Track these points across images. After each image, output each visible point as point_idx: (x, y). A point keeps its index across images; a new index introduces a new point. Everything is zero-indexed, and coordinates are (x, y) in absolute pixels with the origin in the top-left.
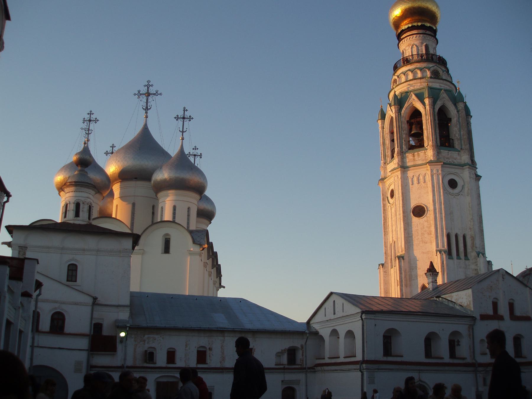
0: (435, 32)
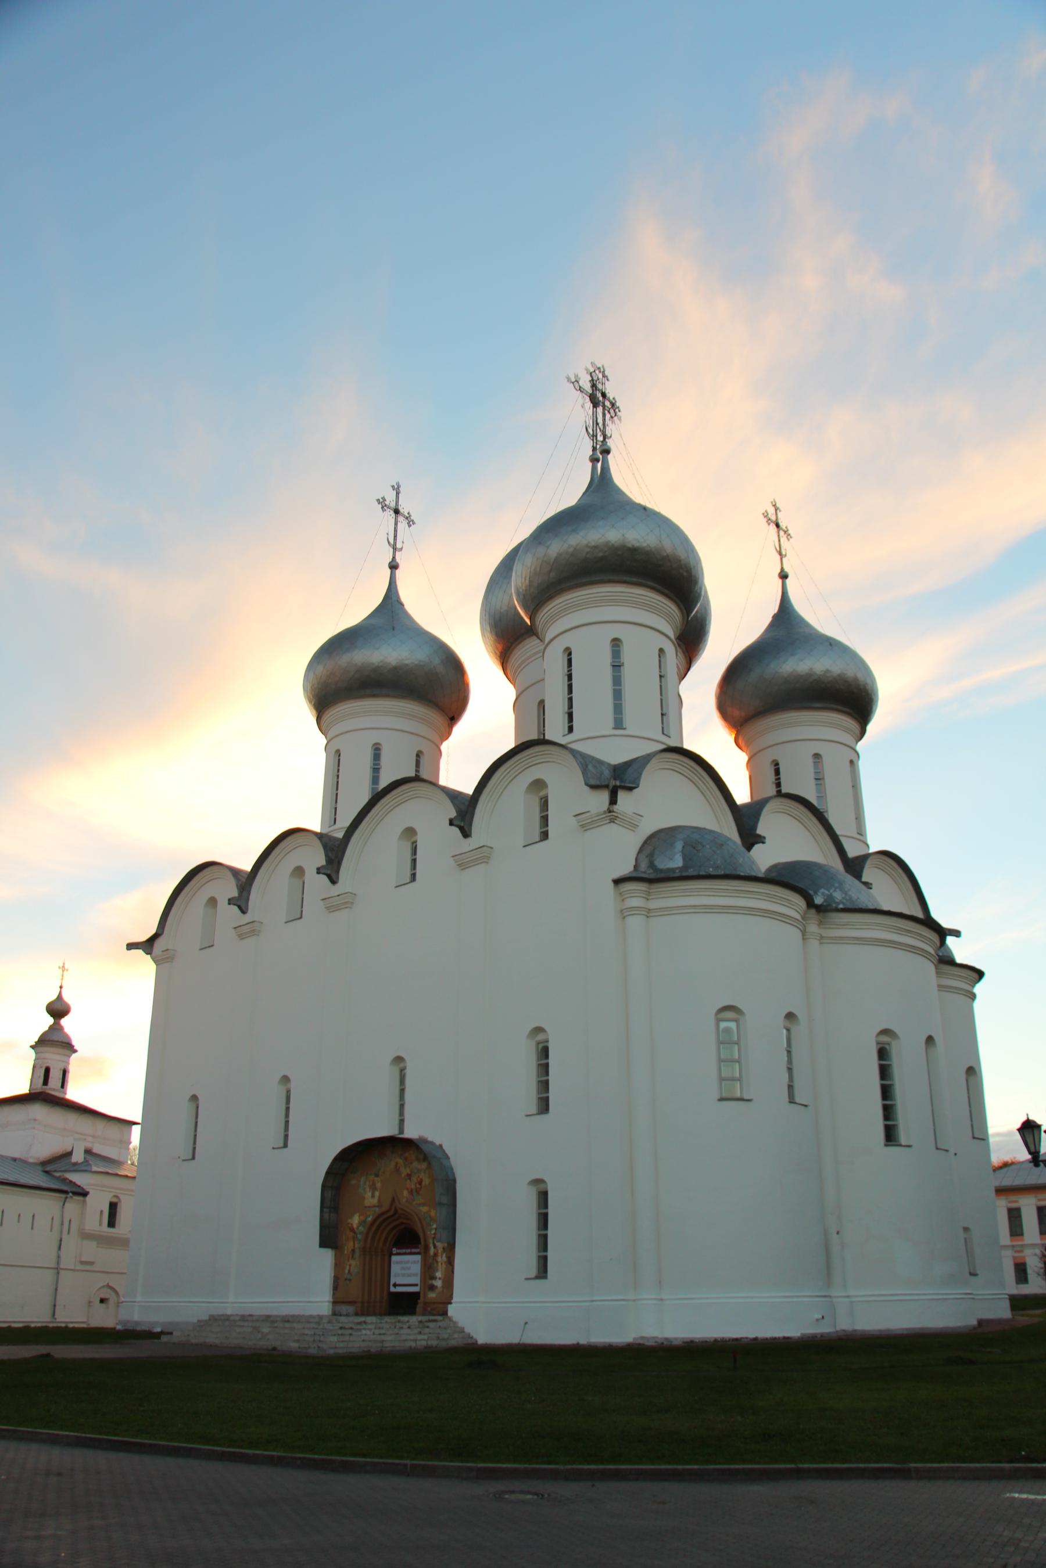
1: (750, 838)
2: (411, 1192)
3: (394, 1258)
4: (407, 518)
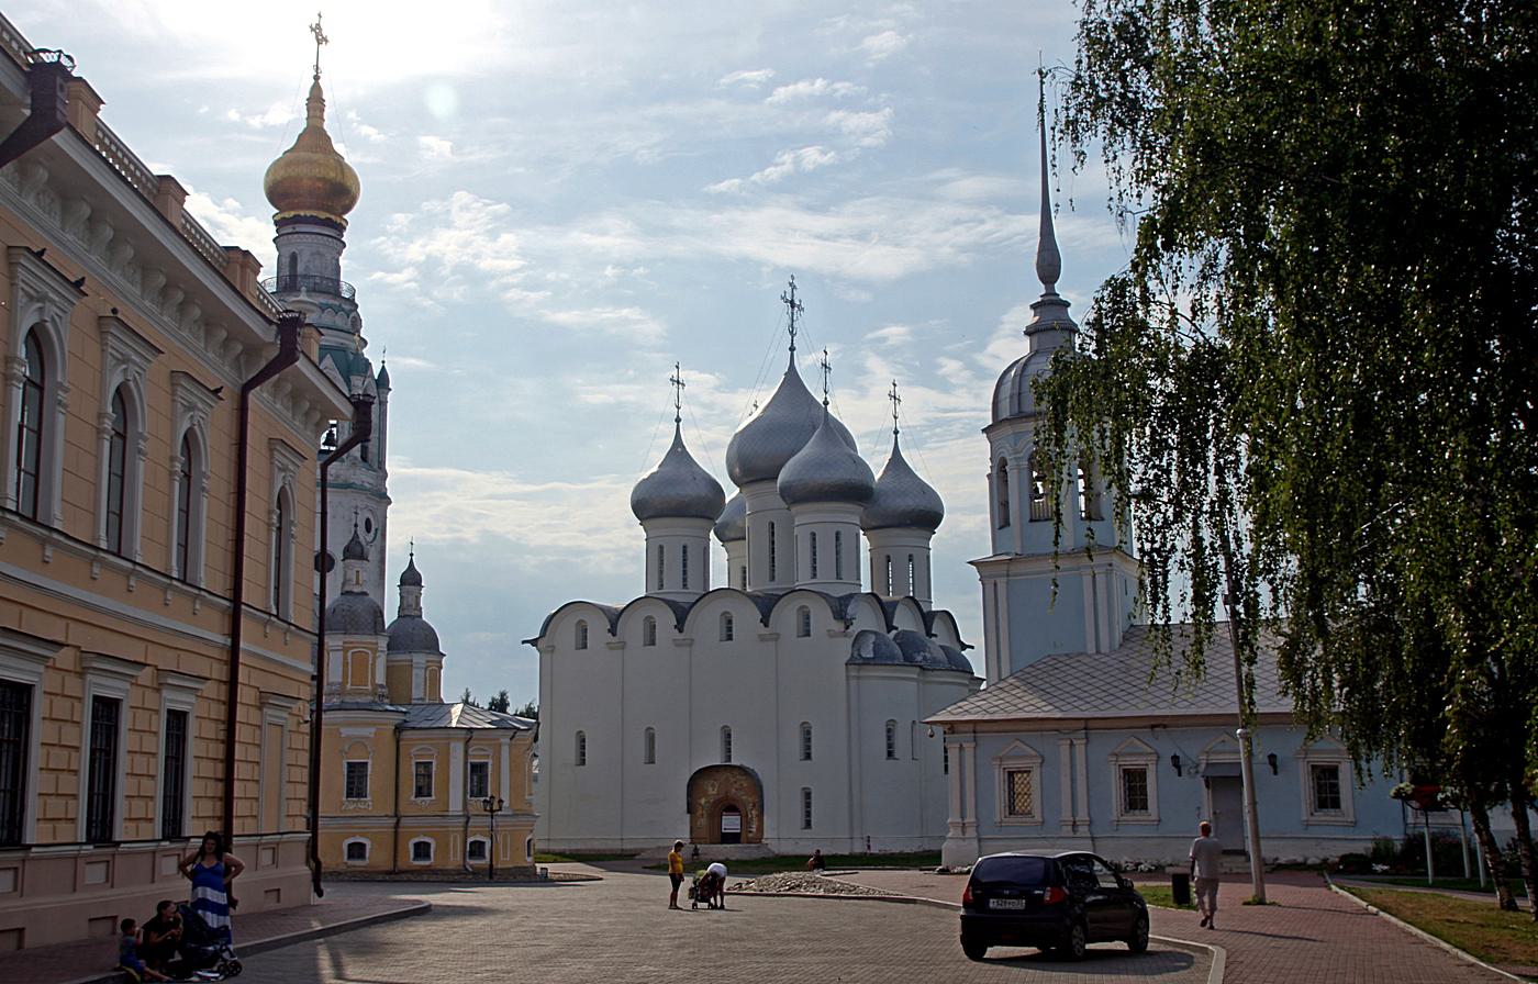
1: (890, 628)
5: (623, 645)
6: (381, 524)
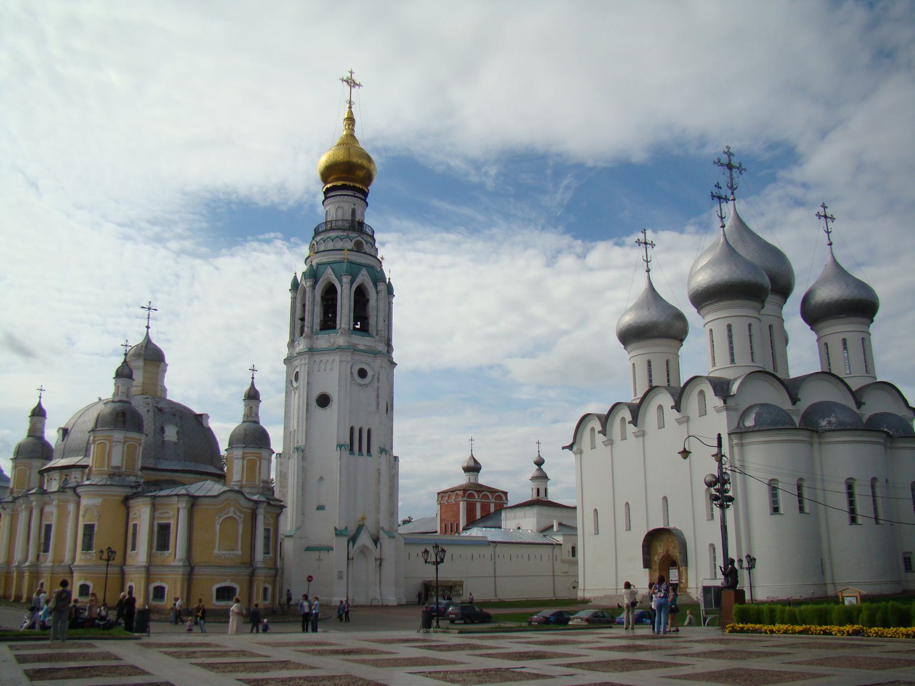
0: (366, 194)
2: (673, 548)
3: (671, 571)
4: (651, 244)
5: (610, 443)
6: (377, 374)
